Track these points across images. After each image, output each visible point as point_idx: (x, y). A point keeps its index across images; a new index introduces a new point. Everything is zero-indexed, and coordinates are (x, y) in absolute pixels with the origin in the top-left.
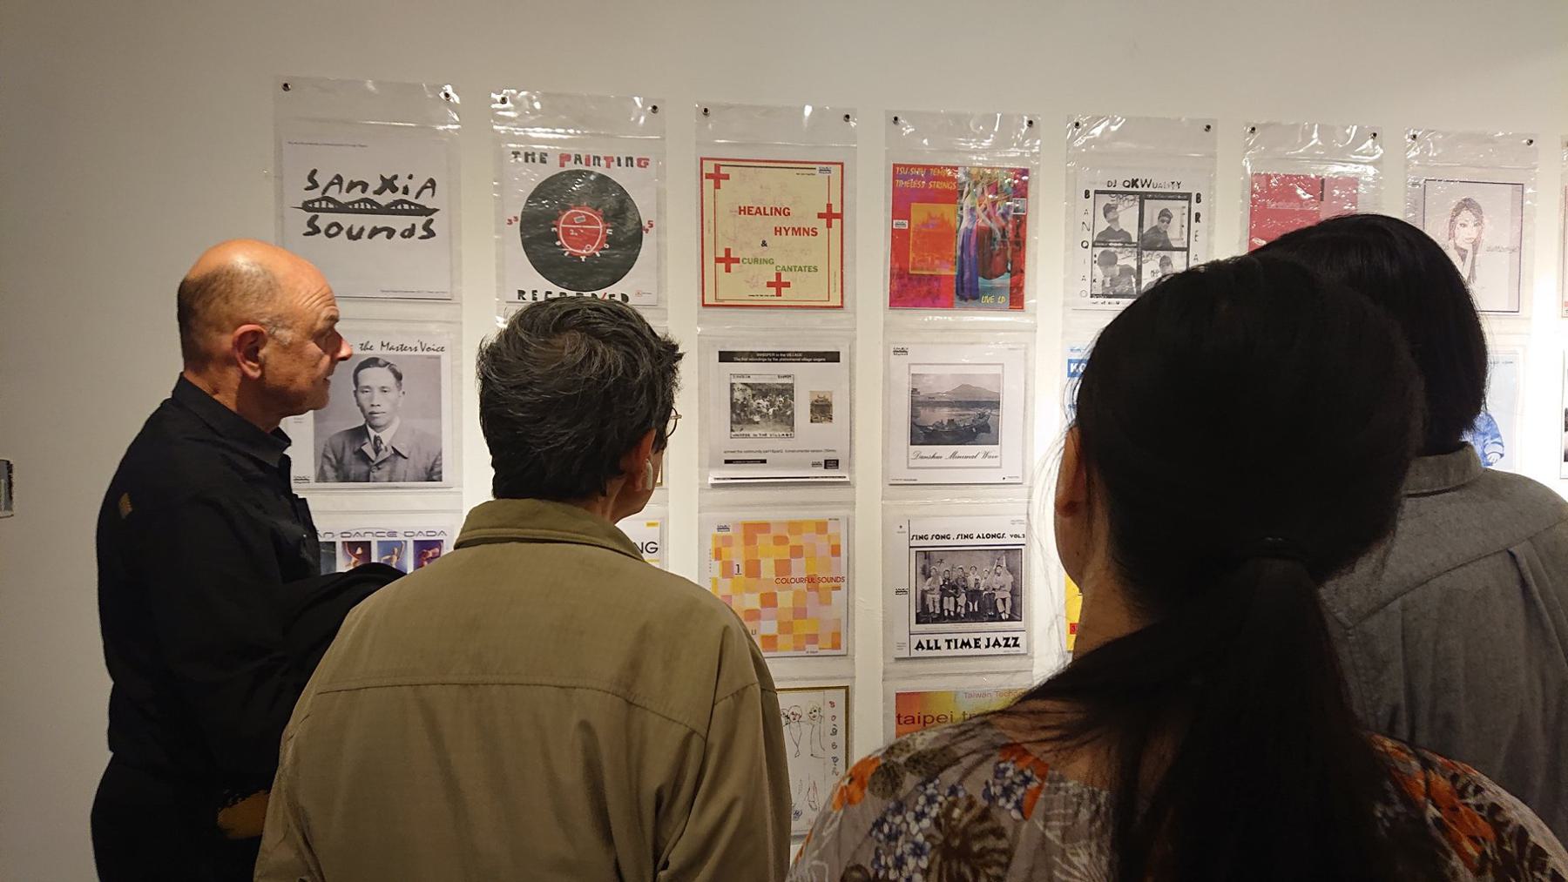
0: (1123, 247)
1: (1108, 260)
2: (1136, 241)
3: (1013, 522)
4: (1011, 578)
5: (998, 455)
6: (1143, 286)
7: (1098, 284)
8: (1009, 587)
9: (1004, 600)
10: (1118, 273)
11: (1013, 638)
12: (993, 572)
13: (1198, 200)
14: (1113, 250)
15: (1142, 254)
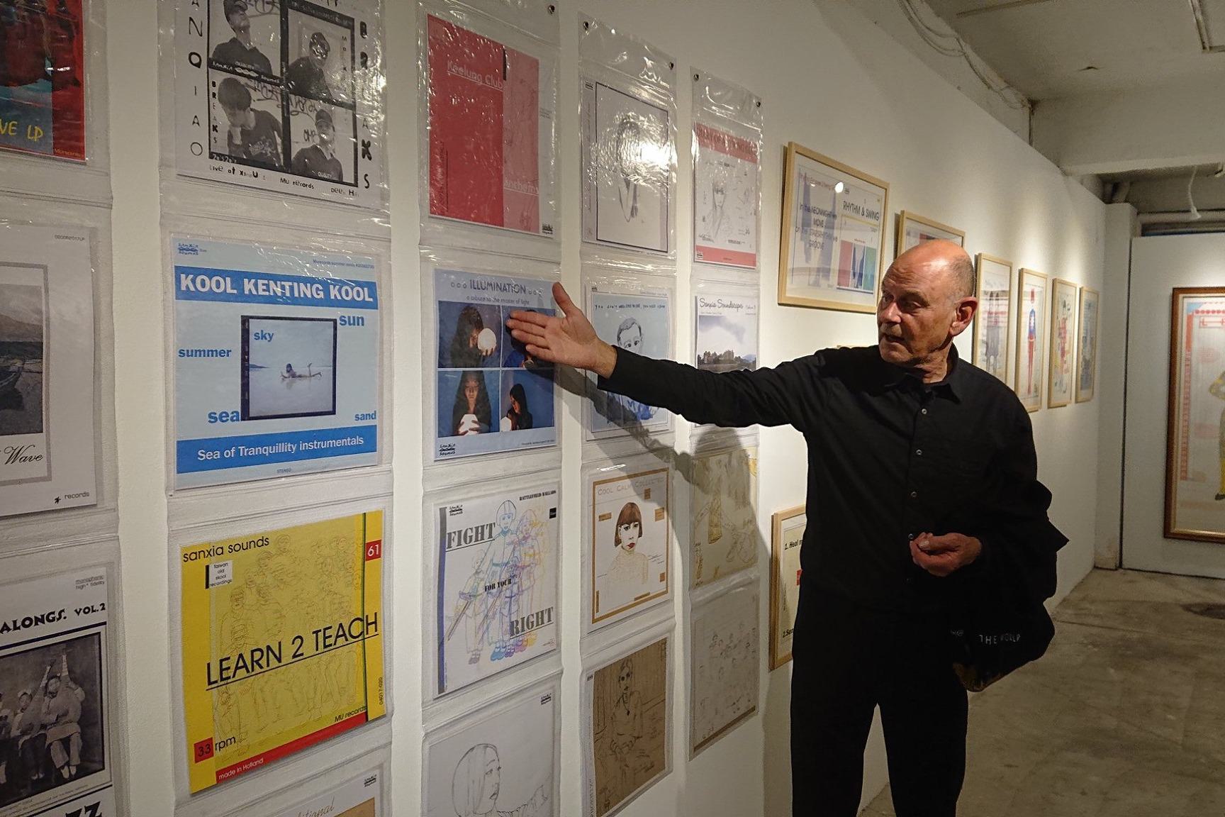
0: (258, 79)
1: (235, 100)
2: (279, 75)
3: (81, 585)
4: (79, 693)
5: (44, 453)
6: (293, 156)
7: (222, 136)
8: (75, 713)
9: (66, 742)
10: (253, 124)
11: (87, 809)
12: (41, 692)
13: (364, 31)
14: (243, 80)
15: (288, 99)
